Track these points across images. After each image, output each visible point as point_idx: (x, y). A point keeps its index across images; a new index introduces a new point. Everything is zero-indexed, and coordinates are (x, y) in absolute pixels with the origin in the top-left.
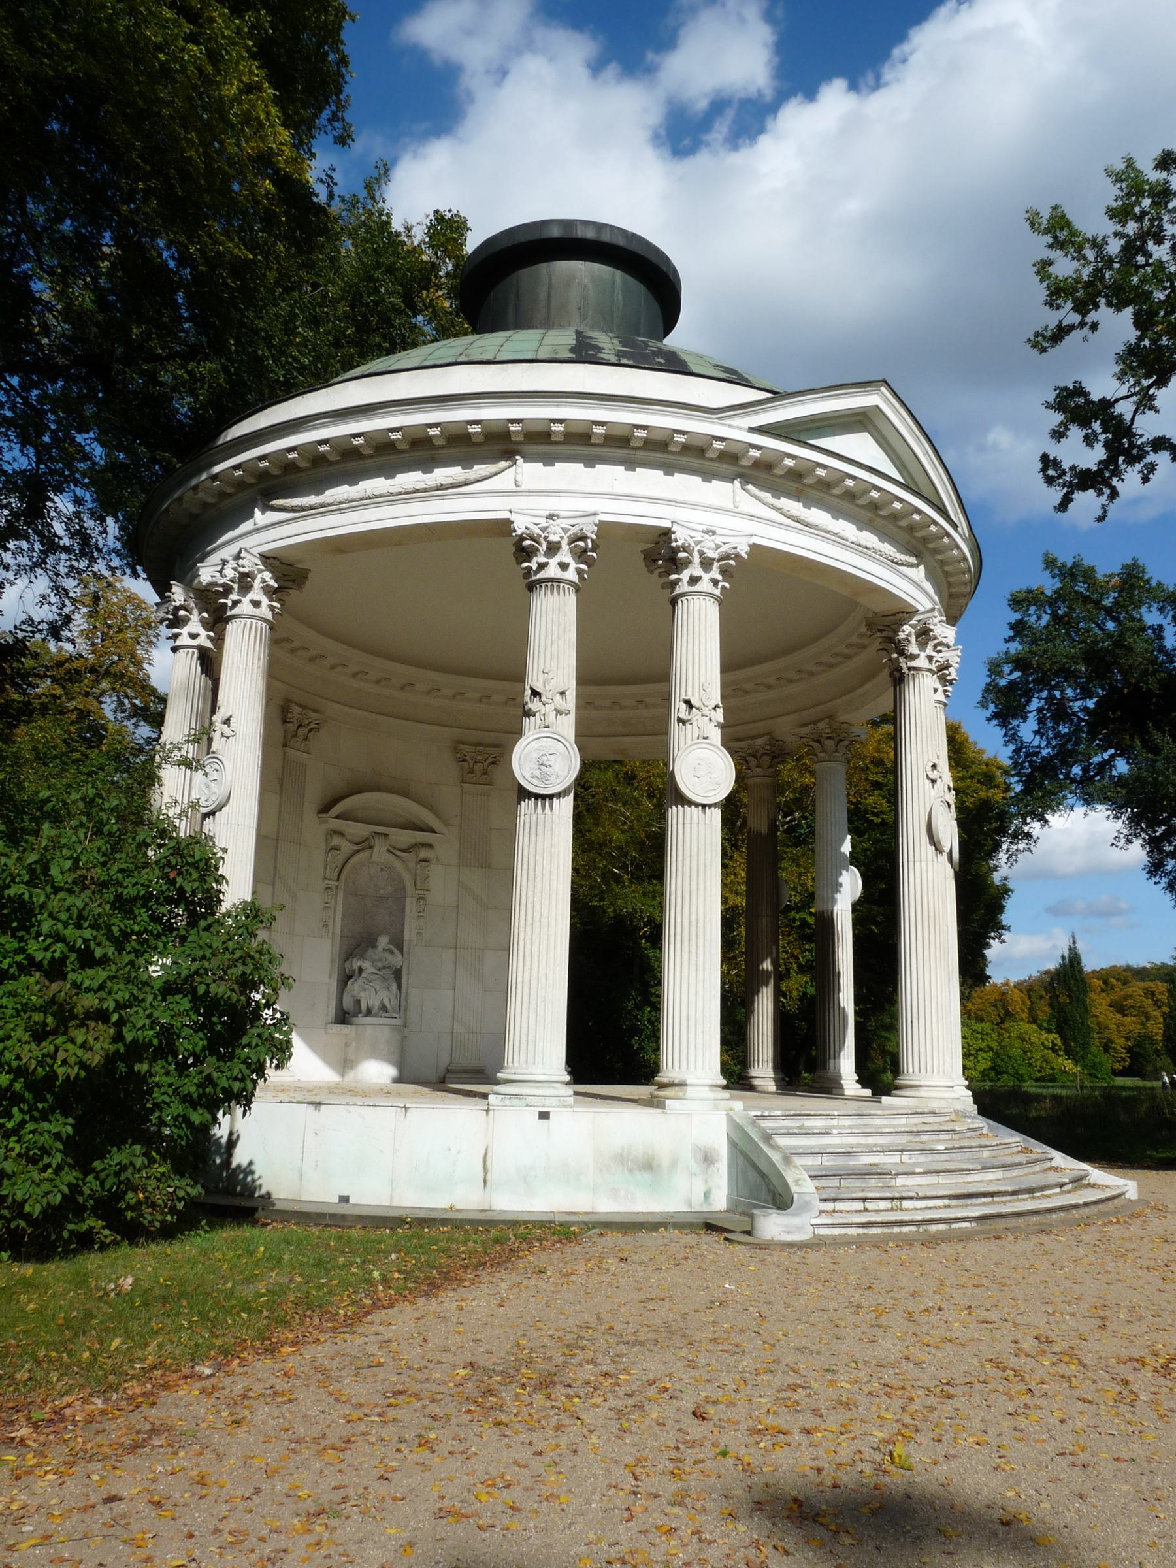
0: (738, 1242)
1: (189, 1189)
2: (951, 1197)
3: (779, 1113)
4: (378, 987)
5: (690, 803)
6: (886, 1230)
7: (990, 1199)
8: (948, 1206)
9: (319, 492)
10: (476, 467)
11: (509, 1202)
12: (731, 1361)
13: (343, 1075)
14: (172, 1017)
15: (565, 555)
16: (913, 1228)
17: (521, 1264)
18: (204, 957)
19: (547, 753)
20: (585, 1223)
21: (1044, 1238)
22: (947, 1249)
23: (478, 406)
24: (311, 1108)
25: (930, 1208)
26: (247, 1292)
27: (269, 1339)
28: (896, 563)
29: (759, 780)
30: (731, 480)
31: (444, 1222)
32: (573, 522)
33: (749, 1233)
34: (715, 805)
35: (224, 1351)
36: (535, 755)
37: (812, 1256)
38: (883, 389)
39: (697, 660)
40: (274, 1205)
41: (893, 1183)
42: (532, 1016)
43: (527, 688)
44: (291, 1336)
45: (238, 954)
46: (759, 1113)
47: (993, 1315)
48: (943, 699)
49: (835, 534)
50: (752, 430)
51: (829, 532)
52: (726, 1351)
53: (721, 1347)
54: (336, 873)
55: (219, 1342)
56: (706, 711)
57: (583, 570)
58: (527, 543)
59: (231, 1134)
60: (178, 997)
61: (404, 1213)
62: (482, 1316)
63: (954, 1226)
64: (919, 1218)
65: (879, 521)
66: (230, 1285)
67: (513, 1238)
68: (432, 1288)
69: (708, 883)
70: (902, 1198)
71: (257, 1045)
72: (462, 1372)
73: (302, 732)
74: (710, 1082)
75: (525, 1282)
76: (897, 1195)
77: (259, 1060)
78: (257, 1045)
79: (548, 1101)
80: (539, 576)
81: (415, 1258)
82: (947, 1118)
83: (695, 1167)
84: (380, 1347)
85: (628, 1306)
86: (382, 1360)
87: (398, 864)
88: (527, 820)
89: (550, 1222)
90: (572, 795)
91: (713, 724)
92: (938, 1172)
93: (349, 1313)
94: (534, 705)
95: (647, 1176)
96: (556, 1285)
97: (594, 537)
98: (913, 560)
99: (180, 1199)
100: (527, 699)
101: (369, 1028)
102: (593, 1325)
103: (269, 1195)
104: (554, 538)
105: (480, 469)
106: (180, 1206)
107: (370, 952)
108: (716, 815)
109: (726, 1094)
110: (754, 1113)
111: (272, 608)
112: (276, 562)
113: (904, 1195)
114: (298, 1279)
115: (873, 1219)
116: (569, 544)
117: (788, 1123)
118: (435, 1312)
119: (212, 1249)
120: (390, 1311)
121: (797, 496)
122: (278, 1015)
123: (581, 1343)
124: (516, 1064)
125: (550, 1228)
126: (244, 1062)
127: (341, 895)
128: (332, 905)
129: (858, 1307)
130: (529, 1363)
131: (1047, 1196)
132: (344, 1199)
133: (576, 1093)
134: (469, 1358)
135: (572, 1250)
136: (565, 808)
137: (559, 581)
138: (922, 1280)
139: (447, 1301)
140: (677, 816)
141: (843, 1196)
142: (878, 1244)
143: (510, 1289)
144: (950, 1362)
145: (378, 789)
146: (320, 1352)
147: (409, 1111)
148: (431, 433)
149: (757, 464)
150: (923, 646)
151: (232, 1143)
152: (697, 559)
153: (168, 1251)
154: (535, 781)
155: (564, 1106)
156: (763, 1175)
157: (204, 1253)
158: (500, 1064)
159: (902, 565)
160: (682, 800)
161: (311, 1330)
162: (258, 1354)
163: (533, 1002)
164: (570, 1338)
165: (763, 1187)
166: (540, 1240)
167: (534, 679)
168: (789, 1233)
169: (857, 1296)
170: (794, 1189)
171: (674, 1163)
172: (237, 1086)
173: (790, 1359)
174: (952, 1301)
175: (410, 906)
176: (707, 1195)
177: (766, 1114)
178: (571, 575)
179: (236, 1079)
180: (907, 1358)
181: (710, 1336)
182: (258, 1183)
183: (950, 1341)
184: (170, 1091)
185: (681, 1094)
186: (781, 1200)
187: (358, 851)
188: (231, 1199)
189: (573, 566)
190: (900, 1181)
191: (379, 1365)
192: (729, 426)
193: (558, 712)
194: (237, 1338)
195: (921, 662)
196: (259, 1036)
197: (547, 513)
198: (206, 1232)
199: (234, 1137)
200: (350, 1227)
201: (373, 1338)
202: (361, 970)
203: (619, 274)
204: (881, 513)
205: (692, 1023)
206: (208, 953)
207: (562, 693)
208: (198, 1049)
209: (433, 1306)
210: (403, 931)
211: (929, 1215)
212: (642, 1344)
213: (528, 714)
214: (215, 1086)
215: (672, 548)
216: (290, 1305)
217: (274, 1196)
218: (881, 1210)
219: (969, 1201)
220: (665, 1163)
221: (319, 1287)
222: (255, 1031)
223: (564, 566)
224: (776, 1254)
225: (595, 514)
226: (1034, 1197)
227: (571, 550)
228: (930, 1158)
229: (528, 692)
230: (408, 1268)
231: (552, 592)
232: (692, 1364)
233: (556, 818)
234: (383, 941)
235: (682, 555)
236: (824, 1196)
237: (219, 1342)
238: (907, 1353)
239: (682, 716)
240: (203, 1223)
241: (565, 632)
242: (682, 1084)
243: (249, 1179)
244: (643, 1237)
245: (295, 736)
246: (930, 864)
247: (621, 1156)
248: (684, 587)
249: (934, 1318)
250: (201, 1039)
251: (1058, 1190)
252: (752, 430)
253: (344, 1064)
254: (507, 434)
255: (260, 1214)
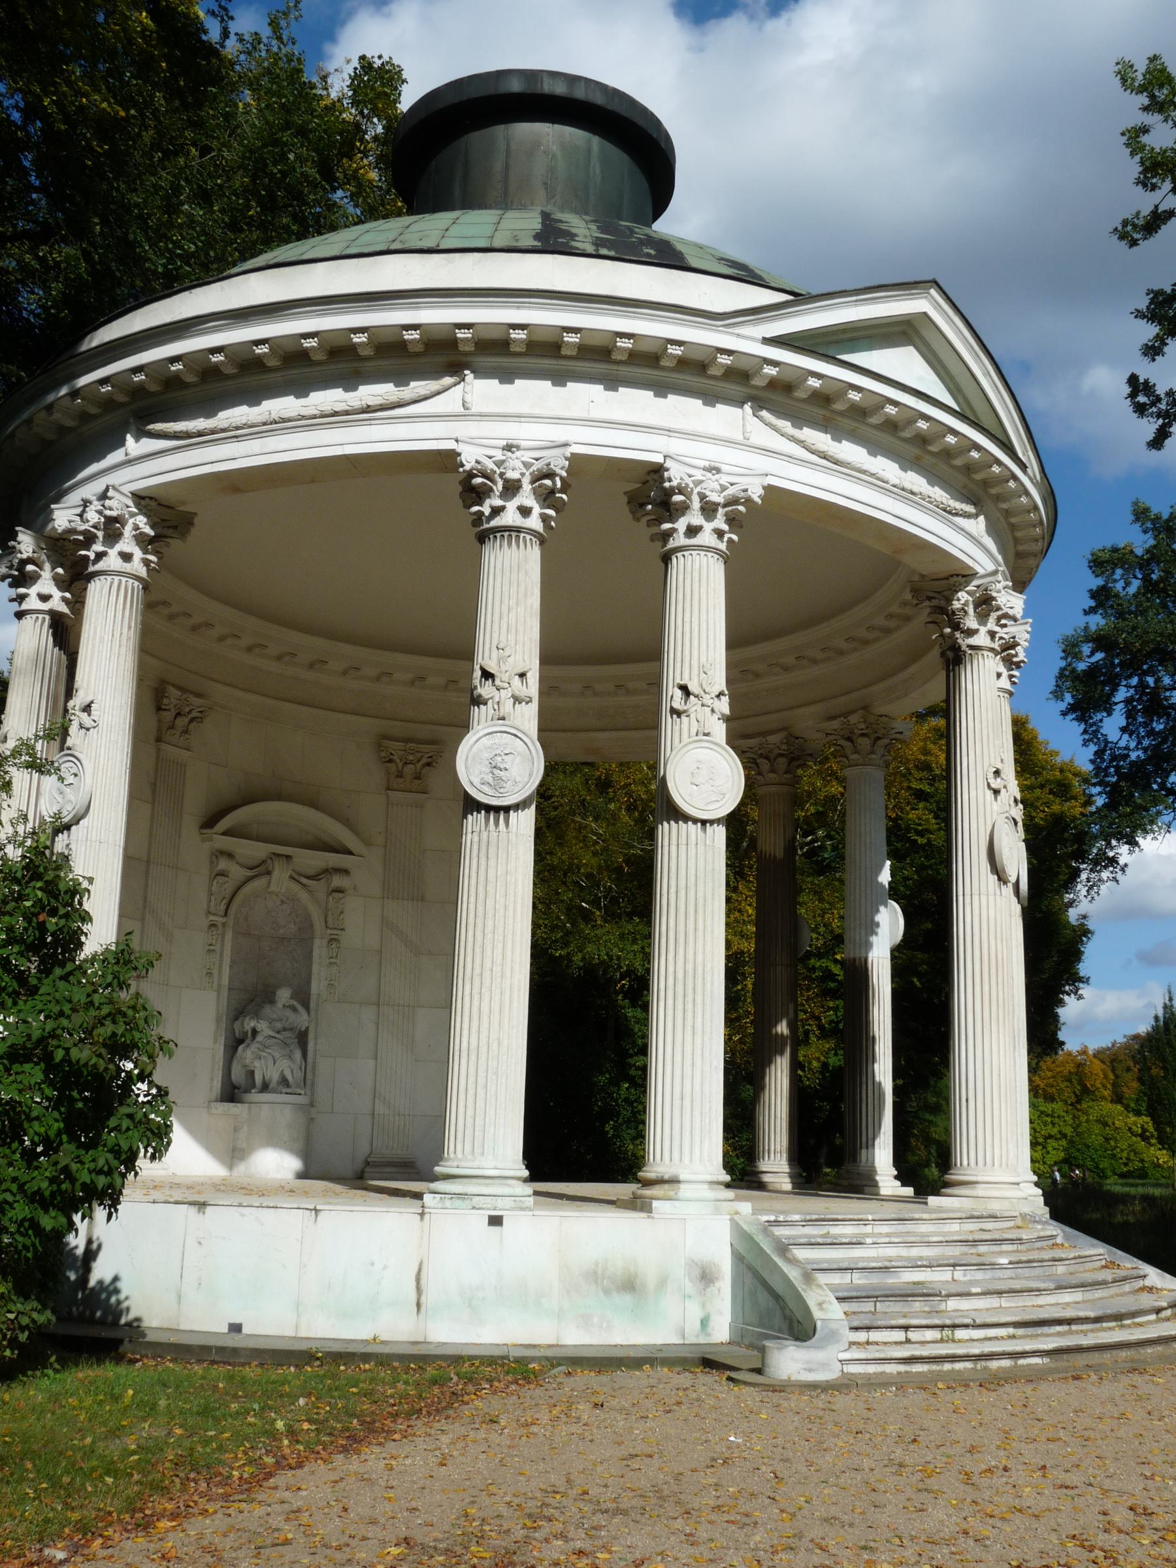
0: (745, 1383)
1: (35, 1315)
2: (1016, 1325)
3: (797, 1217)
4: (277, 1055)
5: (686, 818)
6: (935, 1367)
7: (1065, 1328)
8: (1013, 1337)
9: (210, 414)
10: (413, 384)
11: (448, 1331)
12: (740, 1535)
13: (231, 1167)
14: (20, 1091)
15: (526, 497)
16: (969, 1365)
17: (466, 1411)
18: (61, 1014)
19: (501, 753)
20: (547, 1358)
21: (1136, 1379)
22: (1012, 1391)
23: (417, 307)
24: (193, 1210)
25: (990, 1339)
26: (113, 1449)
27: (142, 1510)
28: (950, 513)
29: (773, 789)
30: (740, 404)
31: (366, 1357)
32: (537, 454)
33: (759, 1371)
34: (718, 821)
35: (83, 1528)
36: (487, 755)
37: (841, 1401)
38: (932, 291)
39: (695, 634)
40: (144, 1336)
41: (943, 1307)
42: (481, 1092)
43: (477, 668)
44: (170, 1506)
45: (105, 1010)
46: (772, 1218)
47: (1074, 1478)
48: (1008, 686)
50: (768, 341)
51: (864, 472)
52: (733, 1522)
53: (726, 1517)
54: (223, 907)
55: (75, 1516)
56: (707, 699)
57: (550, 517)
58: (479, 480)
59: (90, 1242)
60: (27, 1067)
61: (313, 1346)
62: (418, 1476)
63: (1021, 1362)
64: (976, 1351)
65: (928, 460)
66: (89, 1440)
67: (455, 1379)
68: (352, 1443)
69: (709, 923)
70: (955, 1326)
71: (128, 1129)
72: (395, 1551)
73: (181, 722)
75: (472, 1434)
76: (948, 1322)
77: (130, 1148)
78: (128, 1129)
79: (500, 1202)
80: (493, 523)
81: (329, 1404)
82: (1011, 1224)
83: (689, 1287)
84: (287, 1520)
85: (605, 1465)
86: (290, 1536)
87: (303, 895)
88: (476, 839)
89: (503, 1358)
90: (533, 807)
91: (716, 716)
92: (1000, 1293)
93: (246, 1476)
94: (485, 690)
95: (628, 1298)
96: (512, 1437)
97: (564, 474)
98: (970, 509)
99: (23, 1329)
100: (476, 682)
101: (265, 1107)
102: (562, 1489)
103: (138, 1319)
104: (512, 475)
105: (418, 387)
106: (23, 1337)
107: (267, 1010)
108: (719, 834)
109: (730, 1194)
110: (765, 1218)
111: (146, 563)
112: (153, 503)
113: (958, 1321)
114: (179, 1431)
115: (917, 1353)
116: (532, 482)
117: (809, 1230)
118: (356, 1474)
119: (61, 1394)
120: (299, 1472)
121: (824, 425)
122: (154, 1091)
123: (549, 1512)
124: (460, 1154)
125: (503, 1365)
126: (111, 1151)
127: (229, 936)
128: (217, 948)
129: (901, 1465)
130: (481, 1538)
131: (1140, 1325)
132: (236, 1328)
133: (536, 1193)
134: (403, 1532)
135: (532, 1393)
136: (525, 822)
137: (518, 530)
138: (981, 1431)
139: (372, 1459)
140: (669, 834)
141: (879, 1323)
142: (924, 1384)
143: (453, 1443)
144: (1022, 1538)
145: (279, 797)
146: (207, 1526)
147: (321, 1215)
148: (356, 340)
149: (773, 384)
150: (983, 618)
151: (91, 1254)
152: (696, 504)
153: (7, 1397)
154: (486, 789)
155: (521, 1209)
156: (777, 1297)
157: (55, 1398)
158: (438, 1153)
159: (956, 514)
160: (676, 814)
161: (196, 1498)
162: (127, 1531)
163: (482, 1074)
164: (531, 1506)
165: (776, 1313)
166: (490, 1381)
167: (485, 657)
168: (810, 1370)
169: (899, 1451)
170: (817, 1314)
171: (663, 1282)
172: (101, 1181)
173: (815, 1532)
174: (1021, 1459)
175: (319, 950)
176: (704, 1322)
177: (781, 1218)
178: (534, 522)
179: (100, 1172)
180: (966, 1533)
181: (712, 1503)
182: (125, 1305)
183: (1020, 1511)
184: (14, 1187)
185: (672, 1193)
186: (800, 1328)
187: (255, 876)
188: (91, 1328)
189: (537, 511)
190: (952, 1304)
191: (287, 1542)
192: (738, 335)
193: (517, 700)
194: (99, 1510)
195: (981, 639)
196: (130, 1116)
197: (504, 443)
198: (57, 1371)
199: (95, 1246)
200: (243, 1365)
201: (277, 1508)
202: (255, 1032)
203: (596, 140)
204: (931, 448)
205: (687, 1102)
206: (67, 1008)
207: (522, 675)
208: (52, 1133)
209: (354, 1465)
210: (309, 982)
211: (988, 1348)
212: (624, 1513)
213: (478, 701)
214: (72, 1179)
215: (665, 489)
216: (168, 1465)
217: (146, 1324)
218: (927, 1342)
219: (1039, 1330)
220: (651, 1282)
221: (206, 1442)
222: (124, 1110)
223: (525, 511)
224: (794, 1397)
225: (566, 445)
226: (1122, 1326)
227: (534, 491)
228: (989, 1275)
229: (478, 673)
230: (321, 1417)
231: (510, 544)
232: (691, 1539)
233: (512, 837)
234: (284, 995)
235: (678, 498)
236: (856, 1324)
237: (75, 1516)
238: (965, 1526)
239: (676, 705)
240: (53, 1359)
241: (525, 596)
242: (674, 1181)
243: (113, 1299)
244: (621, 1375)
245: (172, 727)
246: (991, 898)
247: (595, 1273)
248: (680, 540)
249: (999, 1481)
250: (56, 1120)
251: (1153, 1317)
252: (768, 341)
253: (233, 1154)
254: (453, 343)
255: (126, 1347)
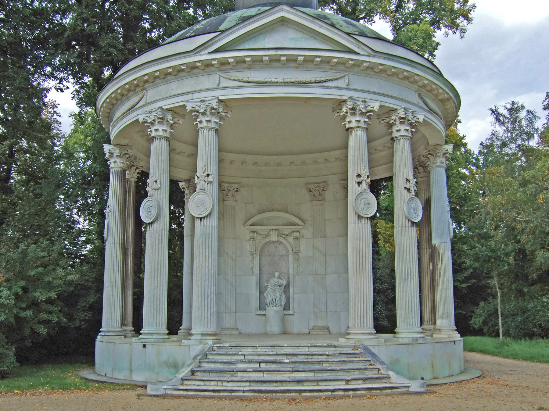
3: (227, 345)
49: (269, 82)
51: (266, 82)
74: (200, 332)
145: (273, 210)
193: (155, 190)
248: (200, 126)
